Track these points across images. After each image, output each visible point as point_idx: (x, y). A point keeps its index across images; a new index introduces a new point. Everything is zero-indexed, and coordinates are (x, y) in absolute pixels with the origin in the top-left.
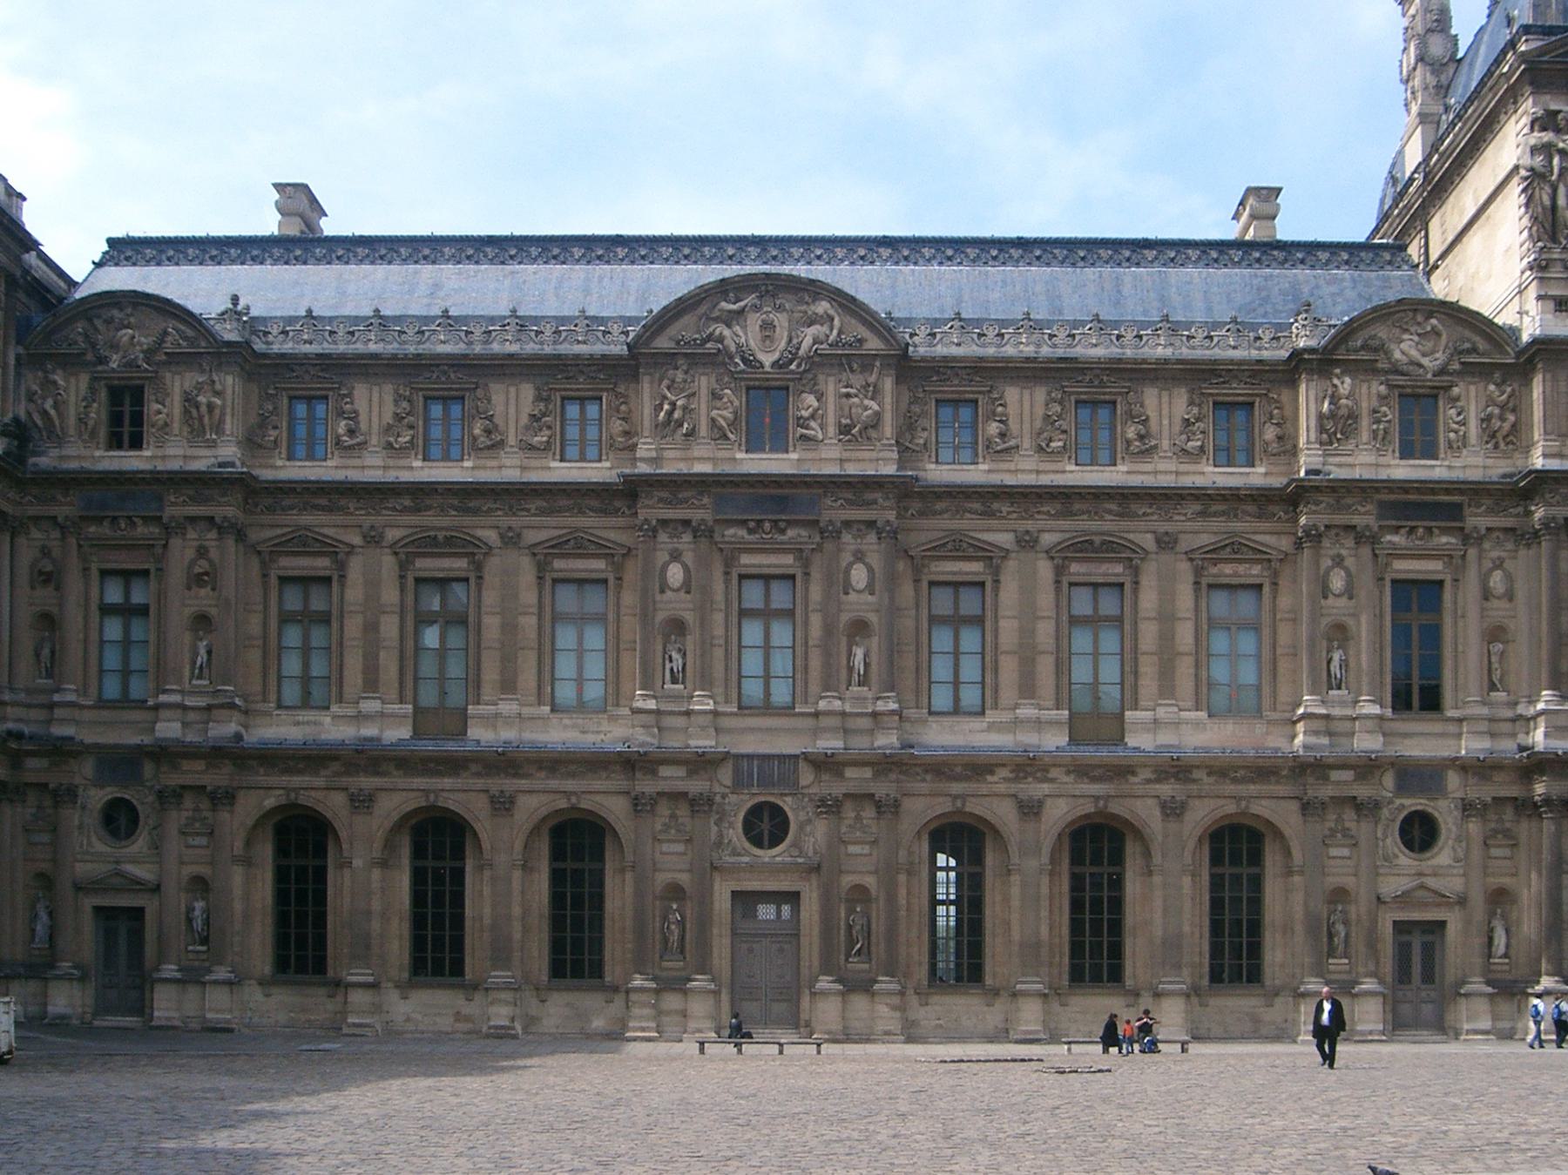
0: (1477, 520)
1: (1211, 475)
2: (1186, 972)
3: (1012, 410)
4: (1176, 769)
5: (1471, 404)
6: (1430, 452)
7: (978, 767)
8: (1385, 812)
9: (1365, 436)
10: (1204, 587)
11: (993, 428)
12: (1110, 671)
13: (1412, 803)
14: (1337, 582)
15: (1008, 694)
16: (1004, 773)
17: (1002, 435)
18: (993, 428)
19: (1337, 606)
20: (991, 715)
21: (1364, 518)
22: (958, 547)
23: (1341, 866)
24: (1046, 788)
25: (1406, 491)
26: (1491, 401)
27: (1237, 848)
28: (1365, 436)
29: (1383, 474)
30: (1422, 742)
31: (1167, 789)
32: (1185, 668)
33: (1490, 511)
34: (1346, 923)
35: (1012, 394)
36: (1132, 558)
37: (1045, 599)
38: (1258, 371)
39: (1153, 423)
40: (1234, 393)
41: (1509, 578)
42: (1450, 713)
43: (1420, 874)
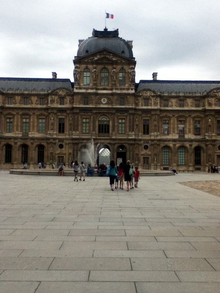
0: (68, 112)
1: (39, 106)
2: (33, 161)
3: (16, 99)
4: (33, 139)
5: (68, 99)
6: (63, 104)
7: (10, 138)
8: (57, 144)
9: (55, 102)
10: (38, 119)
11: (14, 101)
12: (27, 128)
13: (60, 143)
14: (52, 118)
15: (15, 130)
16: (12, 139)
17: (15, 102)
18: (14, 101)
19: (52, 121)
20: (13, 133)
21: (55, 111)
22: (9, 114)
23: (51, 150)
24: (18, 141)
25: (60, 109)
26: (70, 98)
27: (41, 148)
28: (55, 102)
29: (57, 107)
30: (61, 136)
31: (32, 141)
32: (36, 128)
33: (70, 111)
34: (52, 156)
35: (16, 97)
36: (30, 115)
37: (20, 120)
38: (45, 95)
39: (33, 101)
40: (43, 98)
41: (72, 118)
42: (65, 133)
43: (61, 151)
